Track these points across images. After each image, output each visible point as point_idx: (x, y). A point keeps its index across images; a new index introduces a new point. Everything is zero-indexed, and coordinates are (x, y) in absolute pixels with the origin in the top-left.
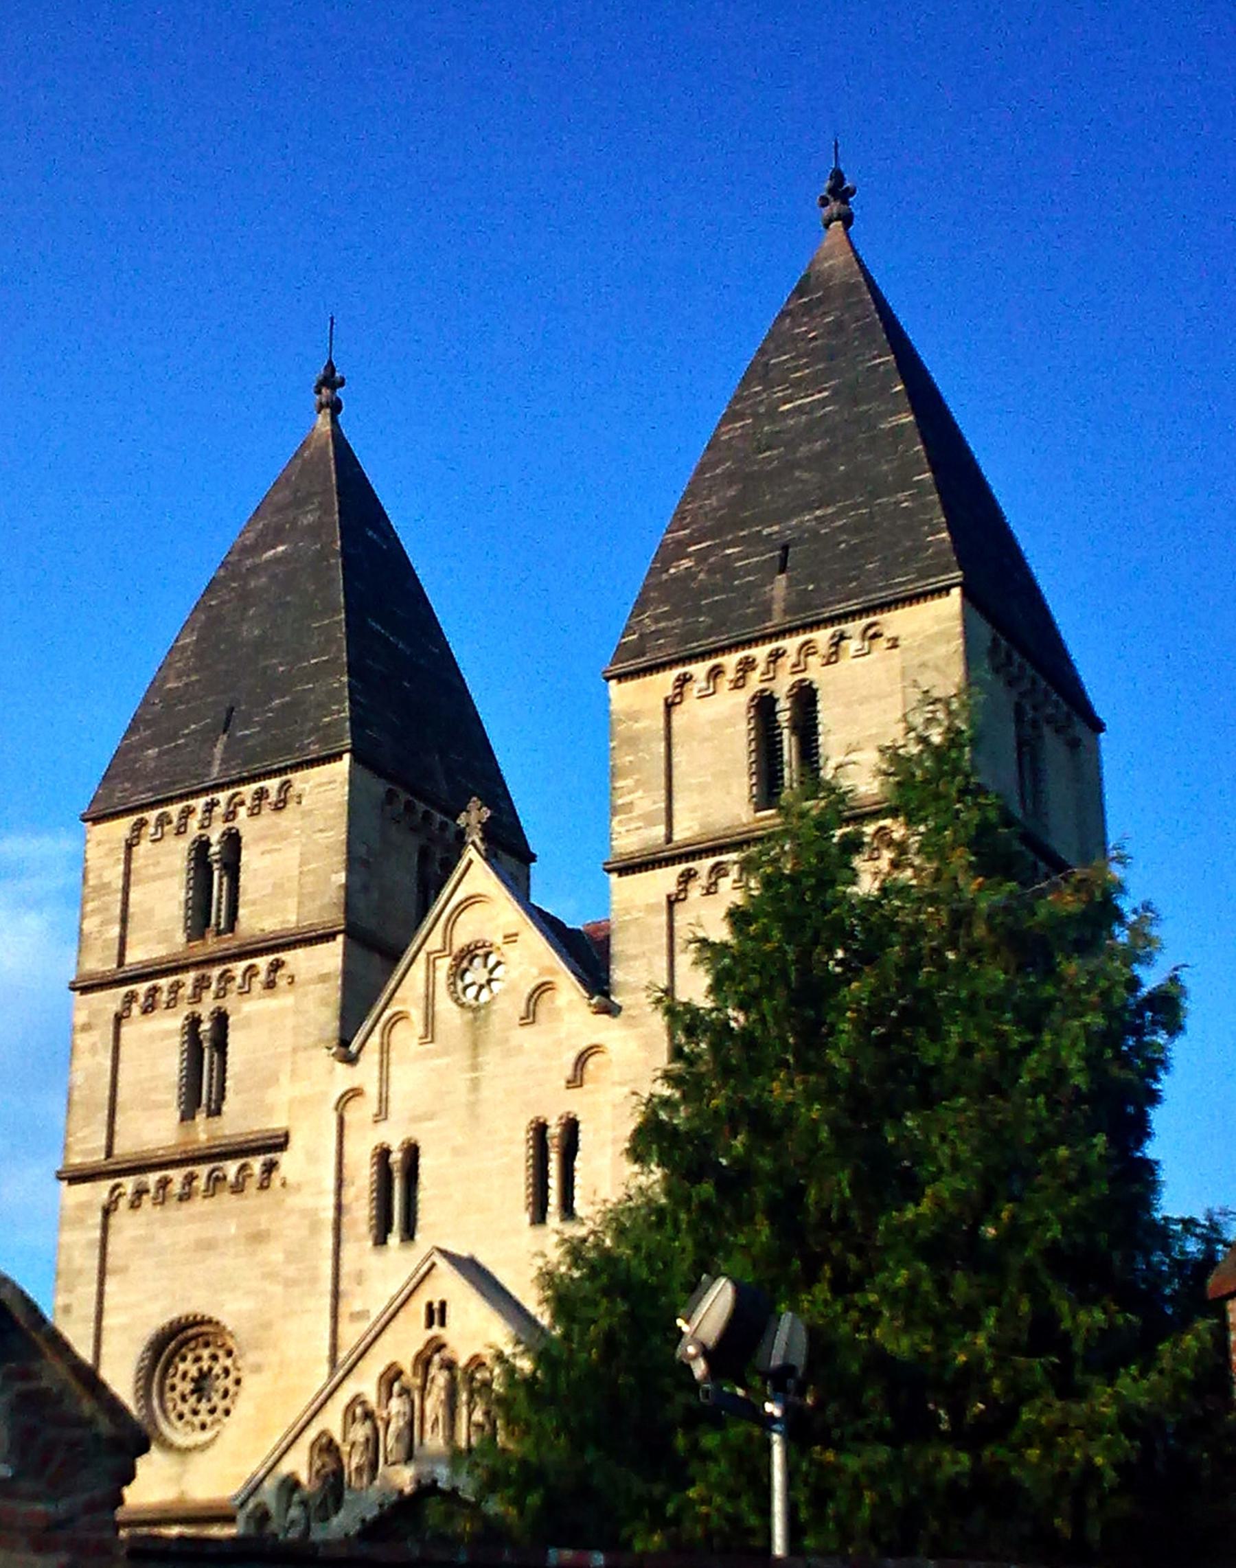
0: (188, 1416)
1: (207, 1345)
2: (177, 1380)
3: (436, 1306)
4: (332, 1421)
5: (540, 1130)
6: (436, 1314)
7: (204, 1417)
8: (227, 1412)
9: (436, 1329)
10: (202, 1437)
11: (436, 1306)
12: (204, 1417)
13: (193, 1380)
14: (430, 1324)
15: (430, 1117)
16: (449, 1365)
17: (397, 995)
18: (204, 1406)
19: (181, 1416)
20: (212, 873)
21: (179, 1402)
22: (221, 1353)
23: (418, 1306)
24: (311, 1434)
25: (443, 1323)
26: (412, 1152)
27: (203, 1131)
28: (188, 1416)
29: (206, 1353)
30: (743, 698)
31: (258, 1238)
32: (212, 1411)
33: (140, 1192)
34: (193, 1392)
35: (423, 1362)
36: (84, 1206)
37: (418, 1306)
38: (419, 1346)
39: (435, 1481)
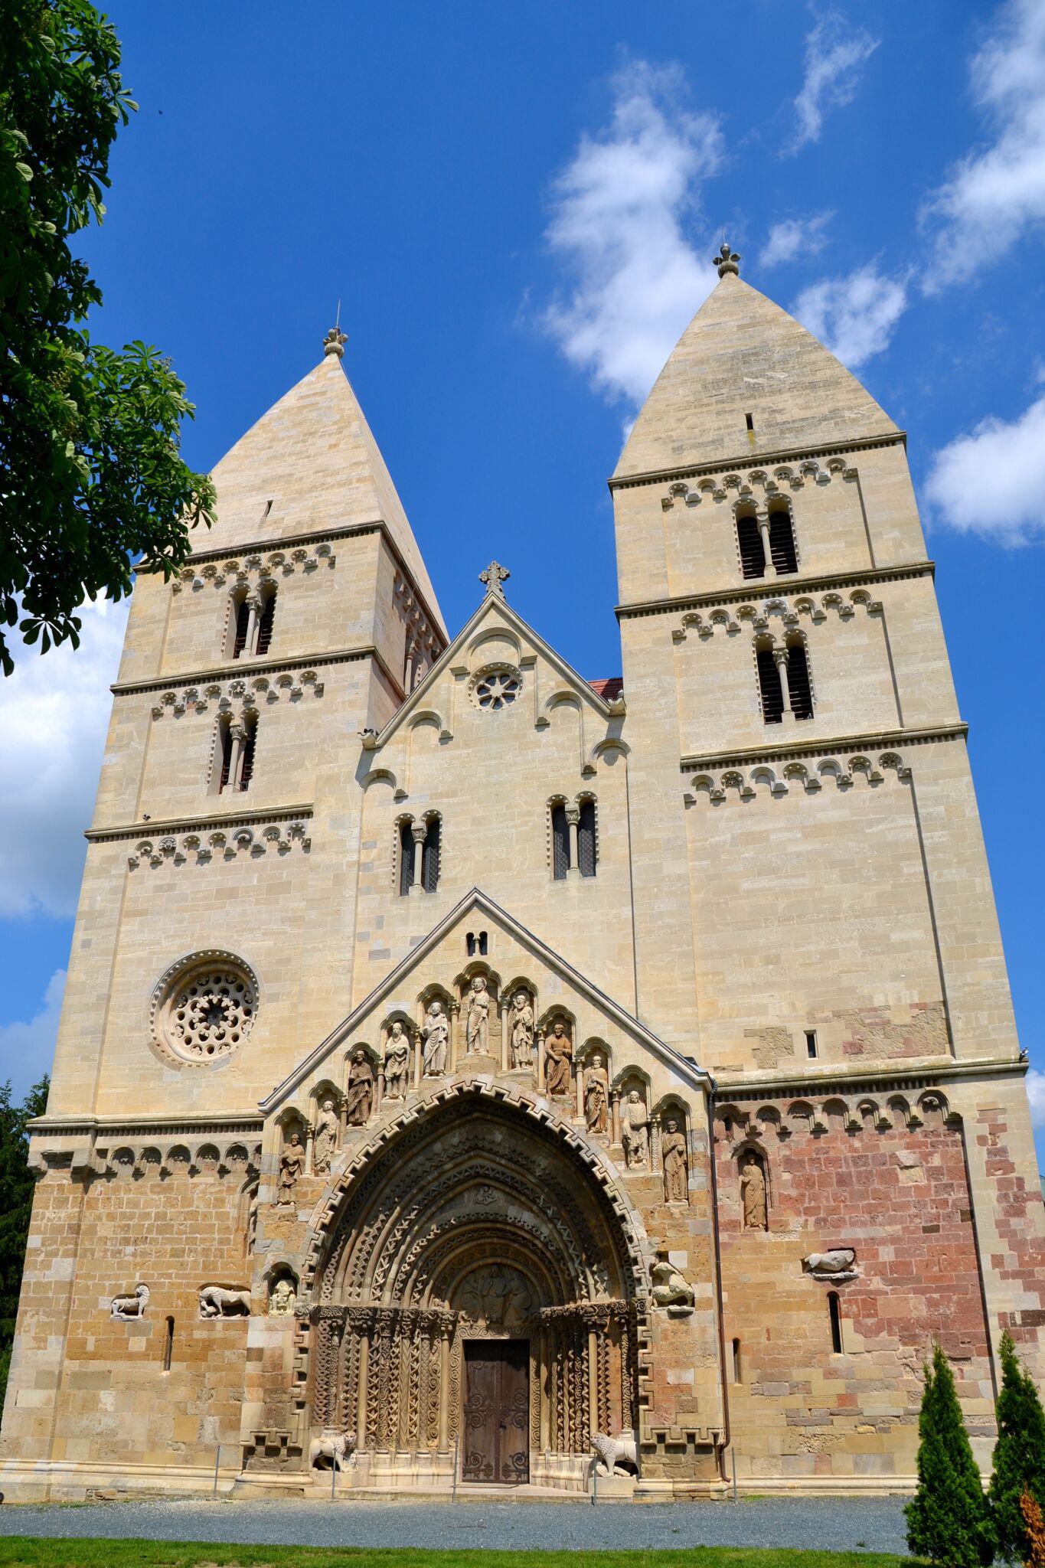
0: (196, 1040)
1: (218, 981)
2: (187, 1009)
3: (477, 936)
4: (371, 1034)
5: (558, 808)
6: (477, 942)
7: (212, 1041)
8: (236, 1038)
9: (477, 957)
10: (206, 1057)
11: (477, 936)
12: (212, 1041)
13: (203, 1010)
14: (471, 952)
15: (453, 794)
16: (493, 982)
17: (422, 700)
18: (214, 1030)
19: (188, 1041)
20: (248, 614)
21: (188, 1029)
22: (231, 988)
23: (459, 935)
24: (347, 1046)
25: (483, 949)
26: (434, 823)
27: (232, 802)
28: (196, 1040)
29: (216, 988)
30: (727, 505)
31: (278, 888)
32: (221, 1037)
33: (168, 850)
34: (201, 1020)
35: (464, 985)
36: (111, 860)
37: (459, 935)
38: (461, 970)
39: (478, 1088)
